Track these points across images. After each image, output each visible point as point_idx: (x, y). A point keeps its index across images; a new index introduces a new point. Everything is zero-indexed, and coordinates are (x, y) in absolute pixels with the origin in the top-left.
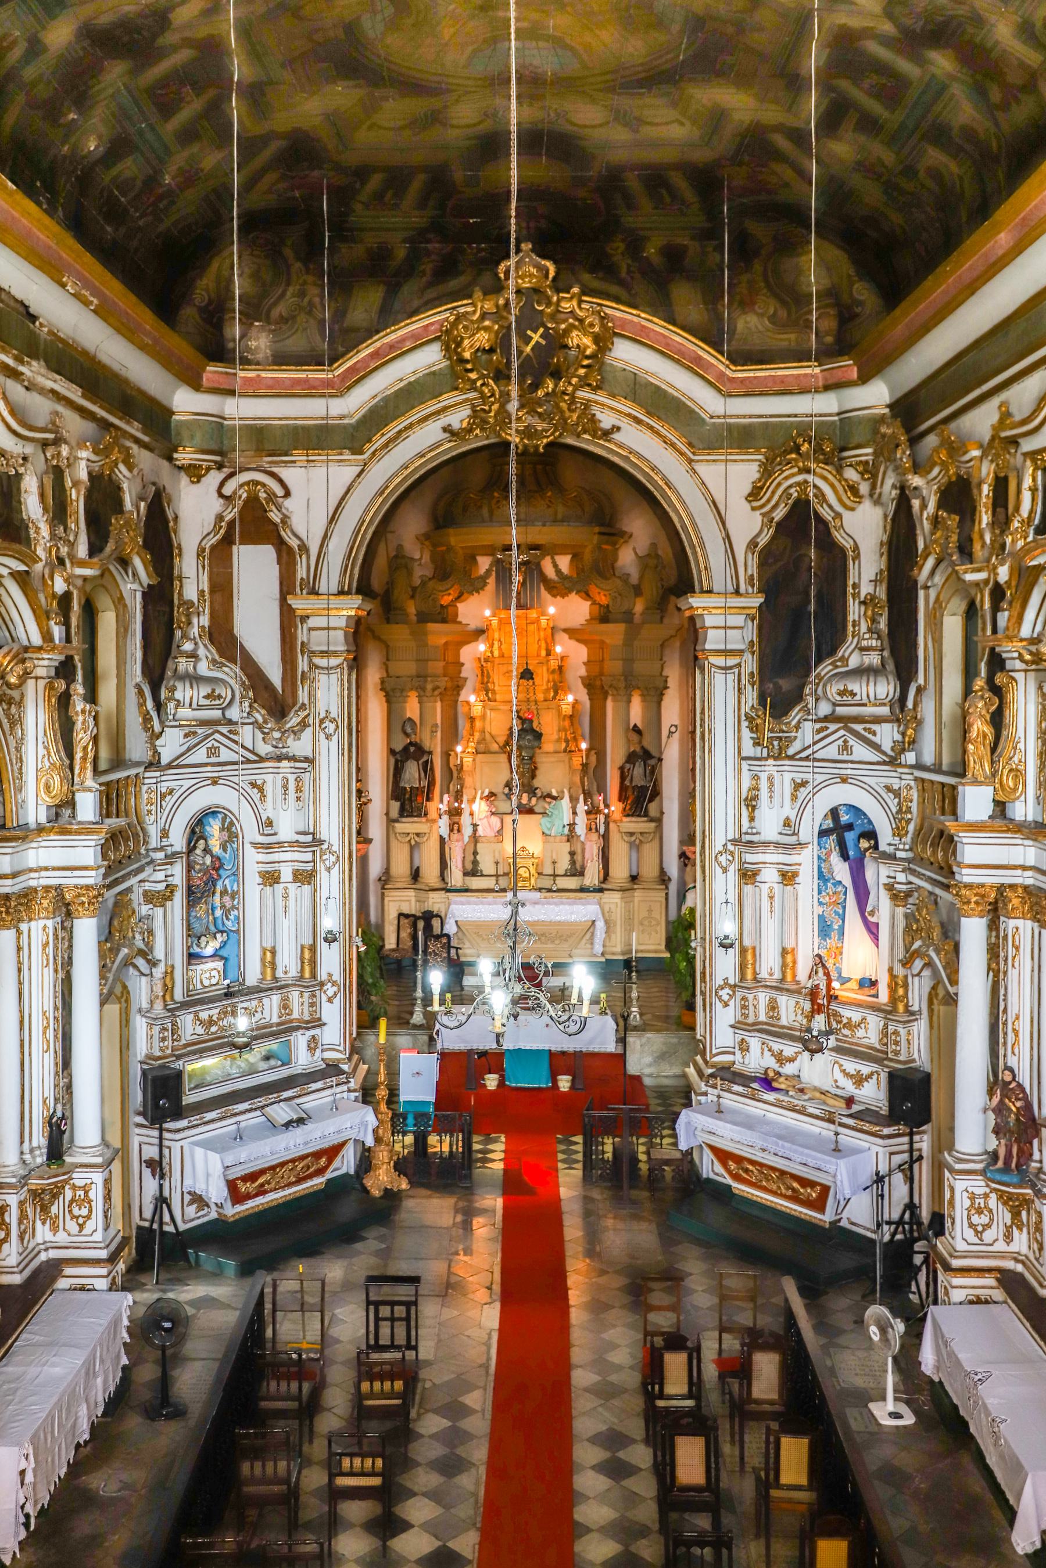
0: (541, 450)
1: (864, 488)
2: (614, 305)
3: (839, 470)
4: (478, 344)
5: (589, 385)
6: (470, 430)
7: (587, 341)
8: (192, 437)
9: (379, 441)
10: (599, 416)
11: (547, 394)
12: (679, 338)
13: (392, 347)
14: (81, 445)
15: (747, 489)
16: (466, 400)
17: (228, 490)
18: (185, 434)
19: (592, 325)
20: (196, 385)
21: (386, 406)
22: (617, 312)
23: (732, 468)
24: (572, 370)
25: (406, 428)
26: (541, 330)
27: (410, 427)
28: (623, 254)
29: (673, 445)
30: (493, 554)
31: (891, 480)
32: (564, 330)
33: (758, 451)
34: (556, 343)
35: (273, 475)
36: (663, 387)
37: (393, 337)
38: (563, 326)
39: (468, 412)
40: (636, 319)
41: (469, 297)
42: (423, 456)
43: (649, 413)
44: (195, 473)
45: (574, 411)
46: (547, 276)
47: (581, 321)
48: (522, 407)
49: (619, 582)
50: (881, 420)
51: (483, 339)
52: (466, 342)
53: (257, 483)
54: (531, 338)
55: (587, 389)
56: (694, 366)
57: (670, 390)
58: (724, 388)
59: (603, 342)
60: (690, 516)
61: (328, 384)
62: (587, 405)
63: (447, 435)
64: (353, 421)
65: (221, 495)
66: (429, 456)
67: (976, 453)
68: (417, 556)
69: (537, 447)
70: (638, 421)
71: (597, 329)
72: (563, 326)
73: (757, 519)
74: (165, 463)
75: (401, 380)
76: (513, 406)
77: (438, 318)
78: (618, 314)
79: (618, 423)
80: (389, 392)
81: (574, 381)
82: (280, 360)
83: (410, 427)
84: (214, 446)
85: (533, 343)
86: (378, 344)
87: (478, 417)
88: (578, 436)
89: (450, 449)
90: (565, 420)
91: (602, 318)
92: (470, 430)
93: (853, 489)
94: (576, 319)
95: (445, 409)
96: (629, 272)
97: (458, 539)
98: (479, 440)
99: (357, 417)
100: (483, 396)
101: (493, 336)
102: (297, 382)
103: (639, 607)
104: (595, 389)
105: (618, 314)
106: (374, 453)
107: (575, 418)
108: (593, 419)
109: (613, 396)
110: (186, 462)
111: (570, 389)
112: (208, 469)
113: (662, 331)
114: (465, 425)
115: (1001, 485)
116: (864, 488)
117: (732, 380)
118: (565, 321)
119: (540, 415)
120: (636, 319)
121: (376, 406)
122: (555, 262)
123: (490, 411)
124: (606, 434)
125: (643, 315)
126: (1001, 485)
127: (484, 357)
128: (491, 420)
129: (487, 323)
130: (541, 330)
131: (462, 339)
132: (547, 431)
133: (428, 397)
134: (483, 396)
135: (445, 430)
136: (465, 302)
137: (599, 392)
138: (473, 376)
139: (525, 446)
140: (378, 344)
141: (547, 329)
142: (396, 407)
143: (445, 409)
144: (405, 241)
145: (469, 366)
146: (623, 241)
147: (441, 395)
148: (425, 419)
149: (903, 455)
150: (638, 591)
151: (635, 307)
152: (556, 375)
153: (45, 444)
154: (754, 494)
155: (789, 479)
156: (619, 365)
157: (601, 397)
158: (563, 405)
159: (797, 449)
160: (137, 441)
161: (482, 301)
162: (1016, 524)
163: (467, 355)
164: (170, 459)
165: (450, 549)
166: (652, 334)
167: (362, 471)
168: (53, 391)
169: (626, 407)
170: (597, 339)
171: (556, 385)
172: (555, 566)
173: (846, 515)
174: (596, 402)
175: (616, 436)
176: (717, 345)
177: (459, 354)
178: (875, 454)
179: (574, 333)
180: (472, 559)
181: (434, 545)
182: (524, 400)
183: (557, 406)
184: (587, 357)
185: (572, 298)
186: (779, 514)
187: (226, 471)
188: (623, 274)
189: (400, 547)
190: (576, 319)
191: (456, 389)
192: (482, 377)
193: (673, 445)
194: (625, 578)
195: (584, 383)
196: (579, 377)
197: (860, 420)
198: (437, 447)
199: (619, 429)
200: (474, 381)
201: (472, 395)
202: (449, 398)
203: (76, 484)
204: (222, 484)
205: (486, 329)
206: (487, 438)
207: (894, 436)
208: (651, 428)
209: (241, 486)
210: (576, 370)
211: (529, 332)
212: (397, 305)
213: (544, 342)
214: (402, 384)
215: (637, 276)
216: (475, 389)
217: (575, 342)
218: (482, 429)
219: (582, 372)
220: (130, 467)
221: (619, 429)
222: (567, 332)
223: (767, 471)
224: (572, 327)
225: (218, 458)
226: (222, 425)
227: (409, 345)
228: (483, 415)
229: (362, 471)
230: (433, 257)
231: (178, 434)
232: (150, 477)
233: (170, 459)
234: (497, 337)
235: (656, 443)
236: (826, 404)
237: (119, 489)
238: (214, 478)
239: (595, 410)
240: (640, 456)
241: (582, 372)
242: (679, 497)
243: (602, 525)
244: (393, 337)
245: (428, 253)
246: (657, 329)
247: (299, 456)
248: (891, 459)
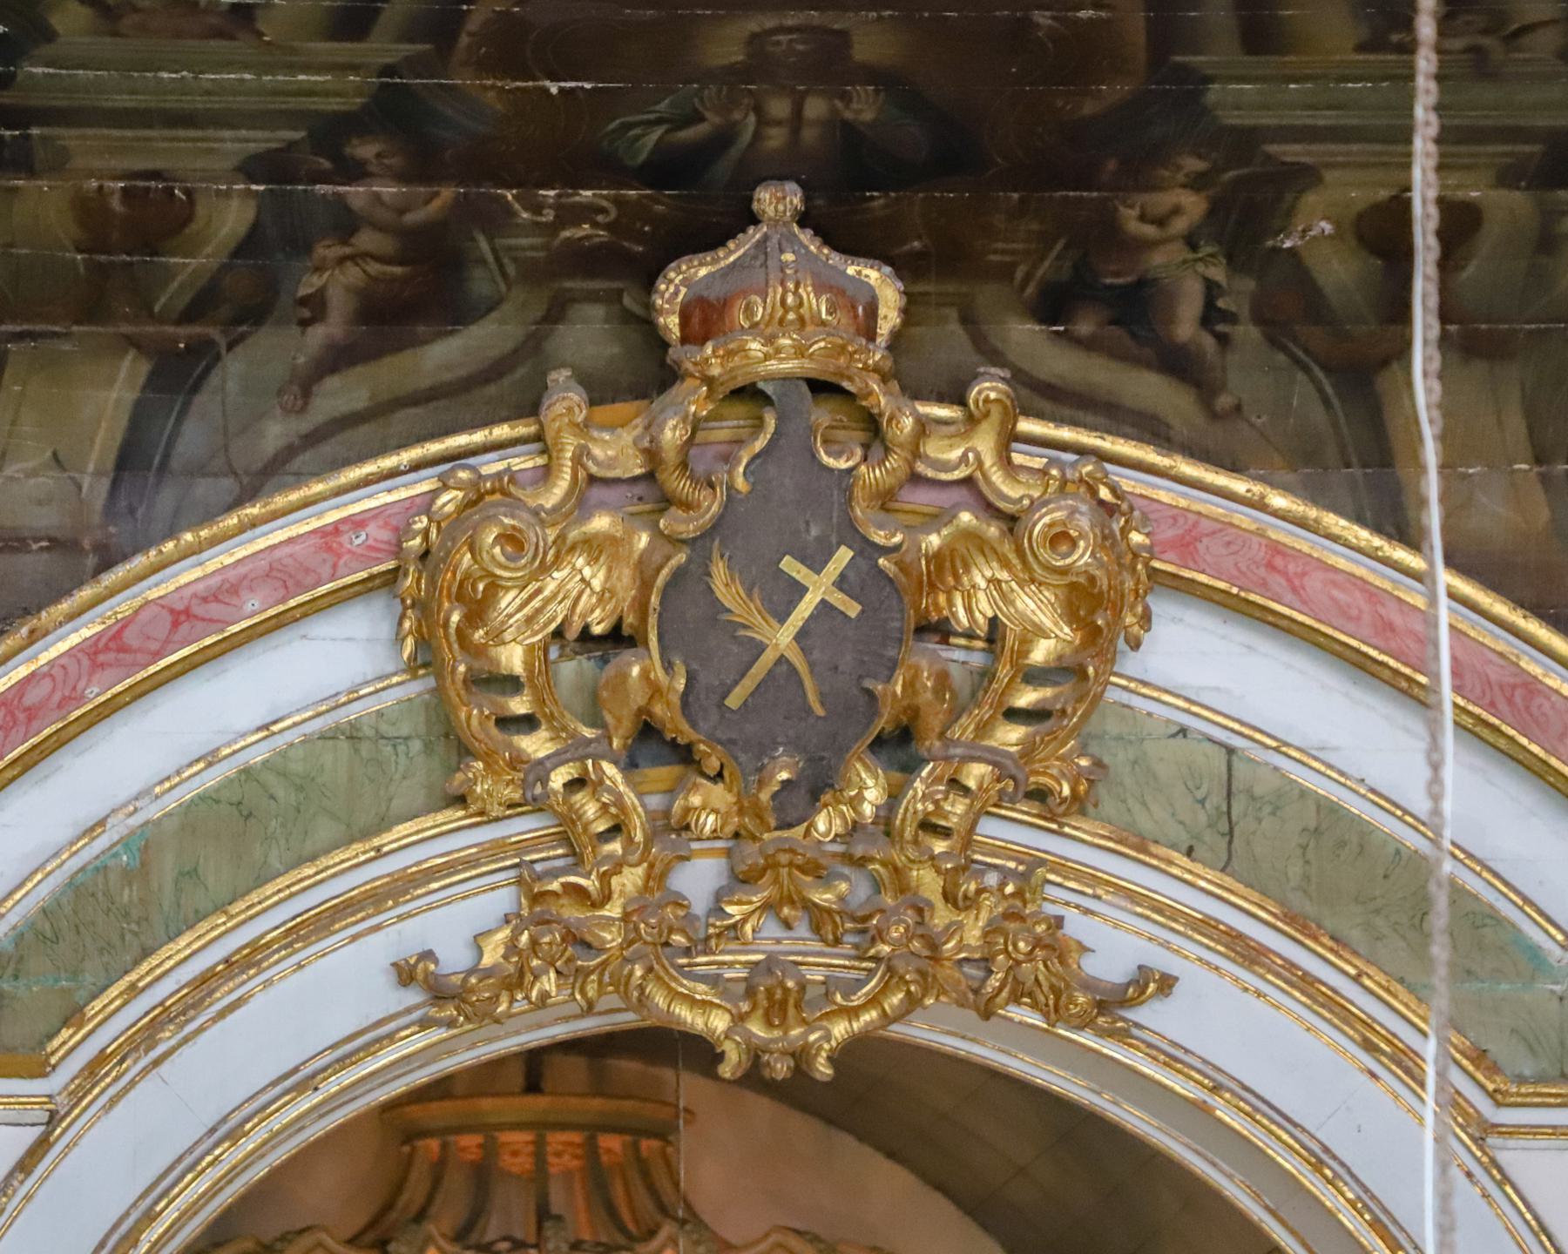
0: (823, 1069)
2: (1150, 455)
4: (559, 611)
5: (1039, 795)
6: (516, 982)
10: (1076, 926)
11: (855, 829)
13: (181, 616)
16: (496, 849)
19: (1060, 538)
21: (139, 873)
24: (964, 729)
25: (234, 966)
26: (844, 555)
28: (1191, 241)
32: (937, 558)
36: (1356, 806)
37: (187, 574)
38: (934, 541)
39: (504, 899)
40: (1244, 518)
41: (530, 407)
42: (308, 1084)
45: (969, 903)
46: (869, 331)
47: (1011, 521)
48: (742, 879)
52: (508, 601)
54: (800, 590)
55: (1025, 810)
57: (1389, 824)
63: (413, 996)
66: (332, 1086)
69: (801, 1057)
70: (1250, 954)
71: (1082, 557)
72: (934, 541)
75: (211, 759)
77: (382, 498)
78: (1165, 493)
79: (1162, 961)
80: (153, 811)
81: (976, 774)
85: (806, 608)
86: (122, 605)
88: (987, 1014)
90: (933, 945)
91: (1109, 509)
92: (516, 982)
94: (989, 509)
95: (402, 886)
96: (1211, 316)
100: (569, 835)
101: (625, 580)
105: (1165, 493)
106: (92, 1070)
107: (973, 934)
108: (1054, 945)
109: (1137, 844)
111: (957, 808)
113: (1362, 569)
114: (492, 955)
118: (936, 519)
119: (819, 918)
120: (1244, 518)
121: (100, 868)
122: (904, 267)
123: (606, 897)
125: (1278, 501)
127: (572, 670)
128: (611, 938)
129: (601, 523)
130: (844, 555)
131: (494, 587)
132: (851, 988)
133: (325, 830)
134: (569, 835)
135: (405, 974)
136: (502, 431)
137: (1079, 826)
138: (536, 745)
139: (756, 1056)
140: (122, 605)
141: (867, 550)
142: (191, 874)
143: (402, 886)
144: (251, 168)
145: (519, 705)
146: (1197, 183)
147: (384, 823)
151: (1234, 467)
158: (928, 882)
161: (584, 428)
163: (513, 658)
166: (1314, 583)
167: (41, 1147)
171: (894, 795)
174: (1061, 867)
175: (1151, 1015)
177: (479, 652)
182: (751, 854)
184: (1034, 677)
185: (972, 421)
188: (1186, 327)
190: (989, 509)
191: (460, 800)
192: (573, 750)
196: (994, 758)
198: (370, 1049)
199: (1167, 984)
200: (541, 770)
201: (523, 827)
205: (594, 547)
206: (589, 1009)
208: (1306, 983)
210: (984, 729)
211: (789, 565)
212: (193, 438)
213: (853, 609)
214: (212, 778)
215: (1247, 333)
216: (537, 805)
217: (984, 607)
218: (572, 976)
221: (1167, 984)
222: (947, 567)
224: (972, 537)
227: (255, 607)
228: (572, 912)
229: (41, 1147)
230: (367, 240)
234: (645, 586)
239: (1058, 899)
241: (1011, 736)
244: (187, 574)
245: (346, 223)
246: (1341, 560)
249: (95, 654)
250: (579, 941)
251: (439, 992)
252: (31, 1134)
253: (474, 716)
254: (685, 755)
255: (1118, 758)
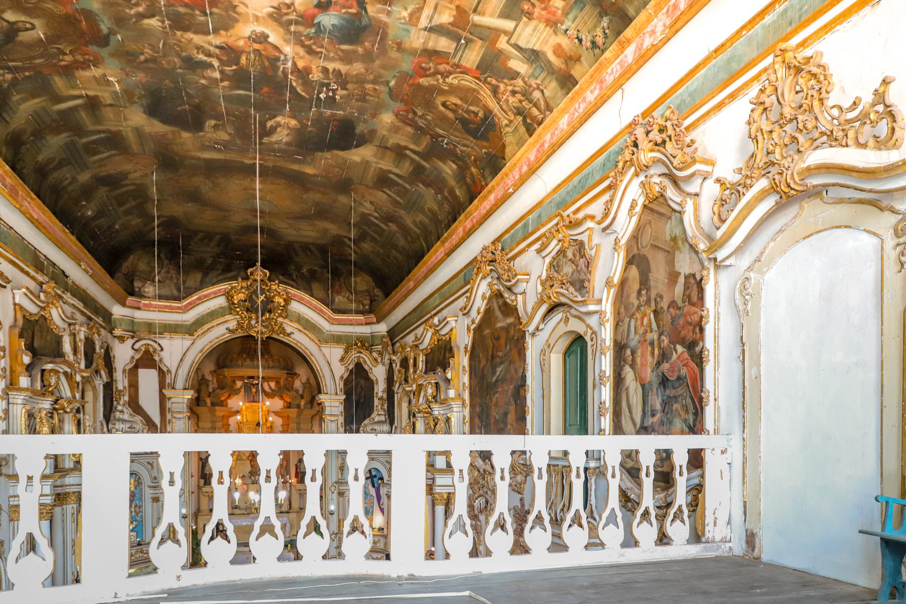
1: (379, 360)
3: (371, 353)
7: (281, 300)
8: (121, 325)
9: (200, 331)
10: (286, 328)
12: (315, 302)
14: (81, 325)
15: (340, 358)
17: (136, 347)
18: (118, 323)
20: (123, 304)
21: (203, 319)
22: (293, 291)
23: (333, 350)
27: (213, 327)
29: (313, 340)
30: (243, 380)
31: (387, 357)
33: (343, 344)
34: (269, 300)
35: (156, 342)
39: (236, 323)
43: (305, 329)
44: (122, 339)
49: (294, 393)
50: (383, 337)
51: (242, 296)
53: (149, 345)
56: (320, 312)
58: (332, 322)
59: (287, 301)
60: (320, 366)
61: (179, 308)
62: (282, 323)
64: (189, 323)
65: (133, 348)
67: (409, 349)
68: (210, 379)
73: (343, 369)
74: (109, 335)
76: (253, 322)
82: (161, 297)
83: (213, 327)
84: (130, 329)
87: (240, 325)
89: (228, 336)
92: (237, 330)
93: (376, 360)
95: (227, 321)
97: (228, 373)
98: (240, 333)
99: (192, 321)
100: (242, 317)
102: (166, 307)
103: (303, 403)
104: (284, 318)
108: (284, 329)
109: (291, 321)
110: (118, 335)
112: (128, 338)
115: (415, 359)
116: (379, 360)
117: (334, 319)
119: (264, 326)
124: (289, 335)
126: (415, 359)
127: (242, 303)
134: (242, 317)
138: (238, 310)
143: (227, 321)
148: (219, 324)
149: (390, 348)
150: (302, 397)
152: (270, 311)
153: (70, 325)
154: (342, 360)
155: (354, 355)
156: (294, 310)
157: (286, 321)
158: (273, 323)
159: (356, 344)
160: (100, 325)
162: (418, 372)
163: (236, 302)
164: (111, 333)
165: (225, 377)
168: (73, 304)
169: (296, 325)
170: (285, 300)
172: (269, 385)
173: (374, 369)
175: (292, 336)
176: (327, 306)
178: (383, 348)
179: (277, 297)
180: (234, 382)
181: (218, 375)
183: (270, 323)
186: (350, 367)
187: (135, 339)
189: (203, 375)
192: (241, 310)
193: (313, 340)
194: (297, 391)
195: (280, 315)
197: (377, 336)
201: (238, 317)
202: (228, 317)
203: (80, 340)
204: (134, 344)
207: (387, 342)
209: (142, 345)
216: (238, 314)
219: (279, 311)
220: (99, 335)
222: (274, 297)
223: (346, 351)
225: (132, 334)
226: (133, 321)
231: (115, 323)
232: (104, 340)
233: (111, 333)
235: (307, 339)
236: (366, 330)
237: (94, 343)
238: (130, 342)
239: (285, 325)
240: (300, 343)
241: (279, 311)
242: (316, 359)
243: (288, 370)
247: (166, 335)
248: (387, 350)
249: (199, 299)
250: (242, 327)
251: (230, 331)
252: (192, 342)
253: (232, 307)
254: (251, 311)
255: (289, 314)
